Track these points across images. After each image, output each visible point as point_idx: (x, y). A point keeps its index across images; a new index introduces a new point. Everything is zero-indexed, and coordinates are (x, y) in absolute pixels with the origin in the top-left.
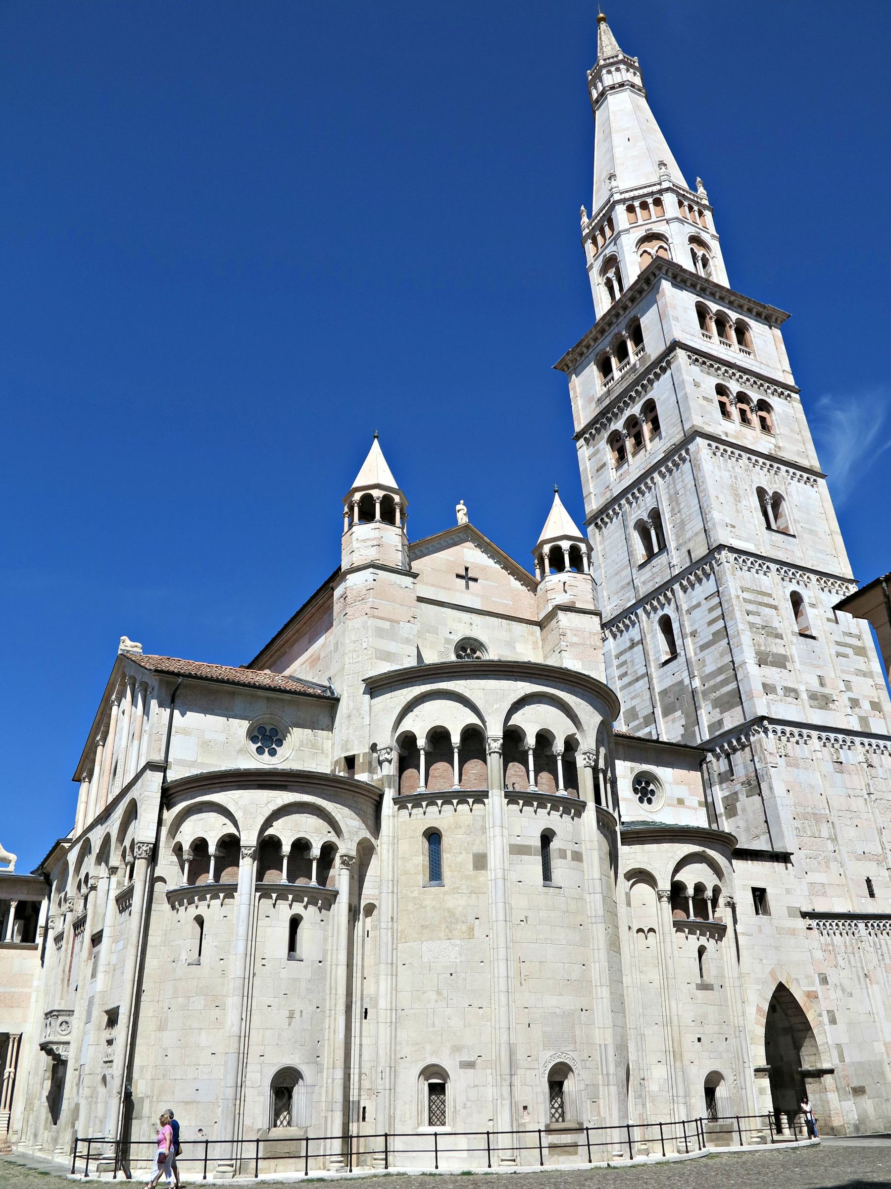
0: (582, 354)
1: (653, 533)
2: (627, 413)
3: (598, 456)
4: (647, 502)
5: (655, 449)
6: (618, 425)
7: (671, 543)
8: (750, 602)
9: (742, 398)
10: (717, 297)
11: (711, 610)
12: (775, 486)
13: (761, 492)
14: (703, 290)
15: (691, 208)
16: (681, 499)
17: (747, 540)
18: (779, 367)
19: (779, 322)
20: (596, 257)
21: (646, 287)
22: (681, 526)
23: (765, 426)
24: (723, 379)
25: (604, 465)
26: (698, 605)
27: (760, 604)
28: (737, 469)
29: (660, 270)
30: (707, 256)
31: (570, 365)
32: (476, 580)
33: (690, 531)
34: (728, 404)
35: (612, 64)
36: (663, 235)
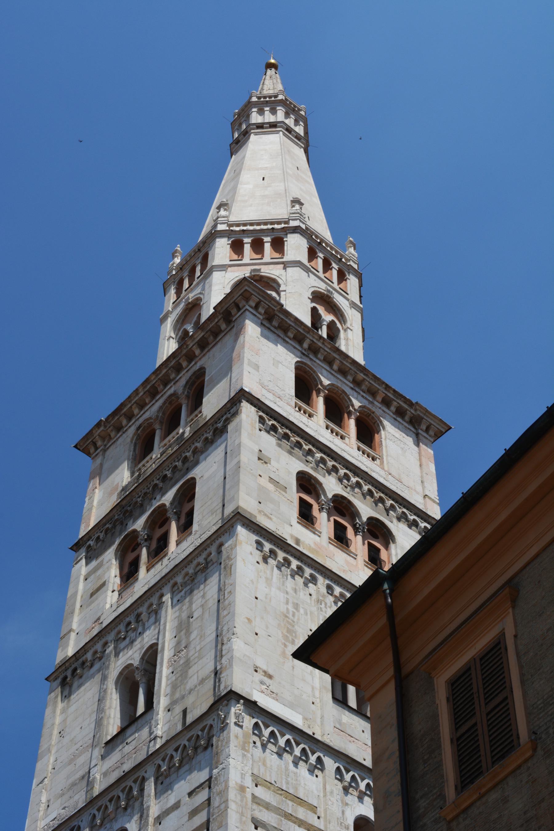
0: (119, 429)
3: (99, 572)
5: (177, 550)
7: (162, 702)
8: (267, 806)
10: (335, 367)
11: (194, 813)
14: (314, 350)
15: (327, 266)
17: (291, 706)
18: (419, 488)
19: (431, 433)
21: (223, 326)
22: (182, 670)
25: (104, 584)
26: (177, 806)
27: (289, 817)
28: (303, 595)
30: (339, 325)
31: (99, 443)
33: (195, 677)
34: (316, 507)
36: (274, 280)
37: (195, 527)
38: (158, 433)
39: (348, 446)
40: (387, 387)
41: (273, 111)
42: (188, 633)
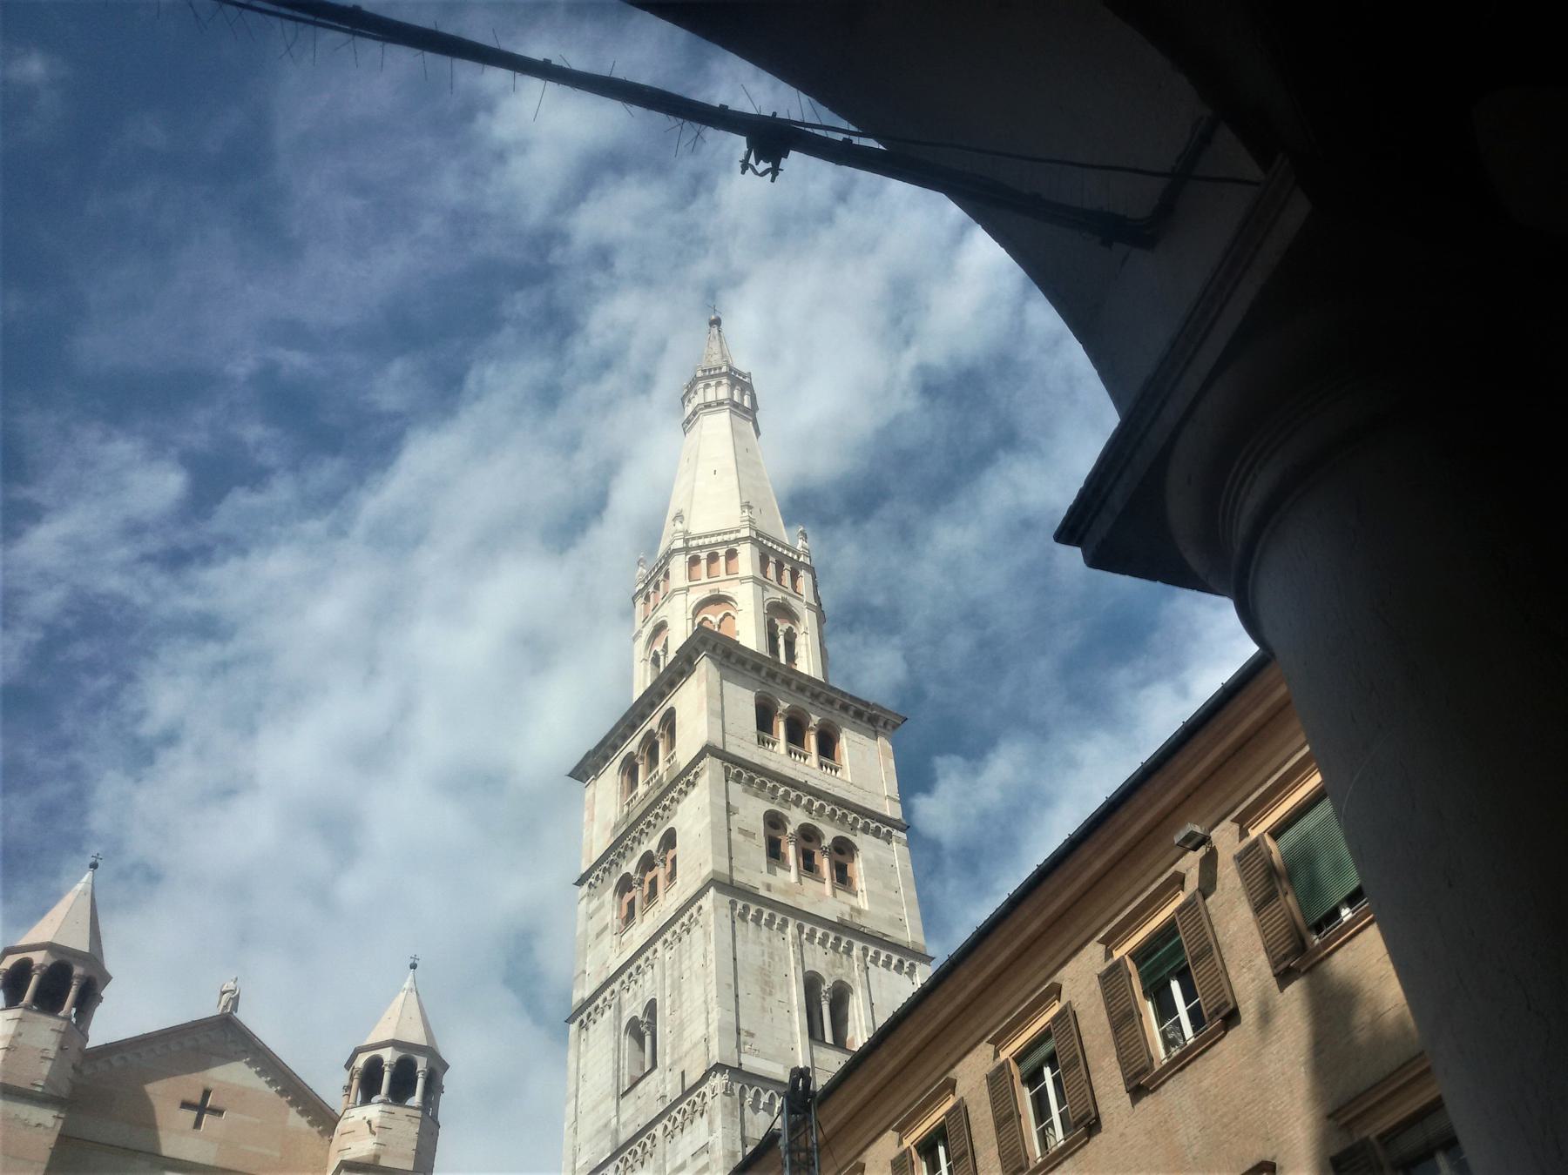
0: (606, 759)
1: (648, 1039)
2: (643, 849)
3: (602, 912)
4: (647, 986)
6: (630, 866)
7: (664, 1060)
9: (808, 835)
10: (793, 687)
12: (840, 971)
13: (812, 983)
14: (772, 675)
16: (685, 987)
20: (646, 620)
21: (687, 668)
23: (842, 878)
24: (780, 805)
25: (606, 928)
28: (777, 942)
29: (710, 644)
32: (218, 1112)
35: (713, 377)
37: (678, 880)
38: (640, 767)
39: (807, 768)
40: (844, 694)
41: (719, 384)
42: (680, 994)
